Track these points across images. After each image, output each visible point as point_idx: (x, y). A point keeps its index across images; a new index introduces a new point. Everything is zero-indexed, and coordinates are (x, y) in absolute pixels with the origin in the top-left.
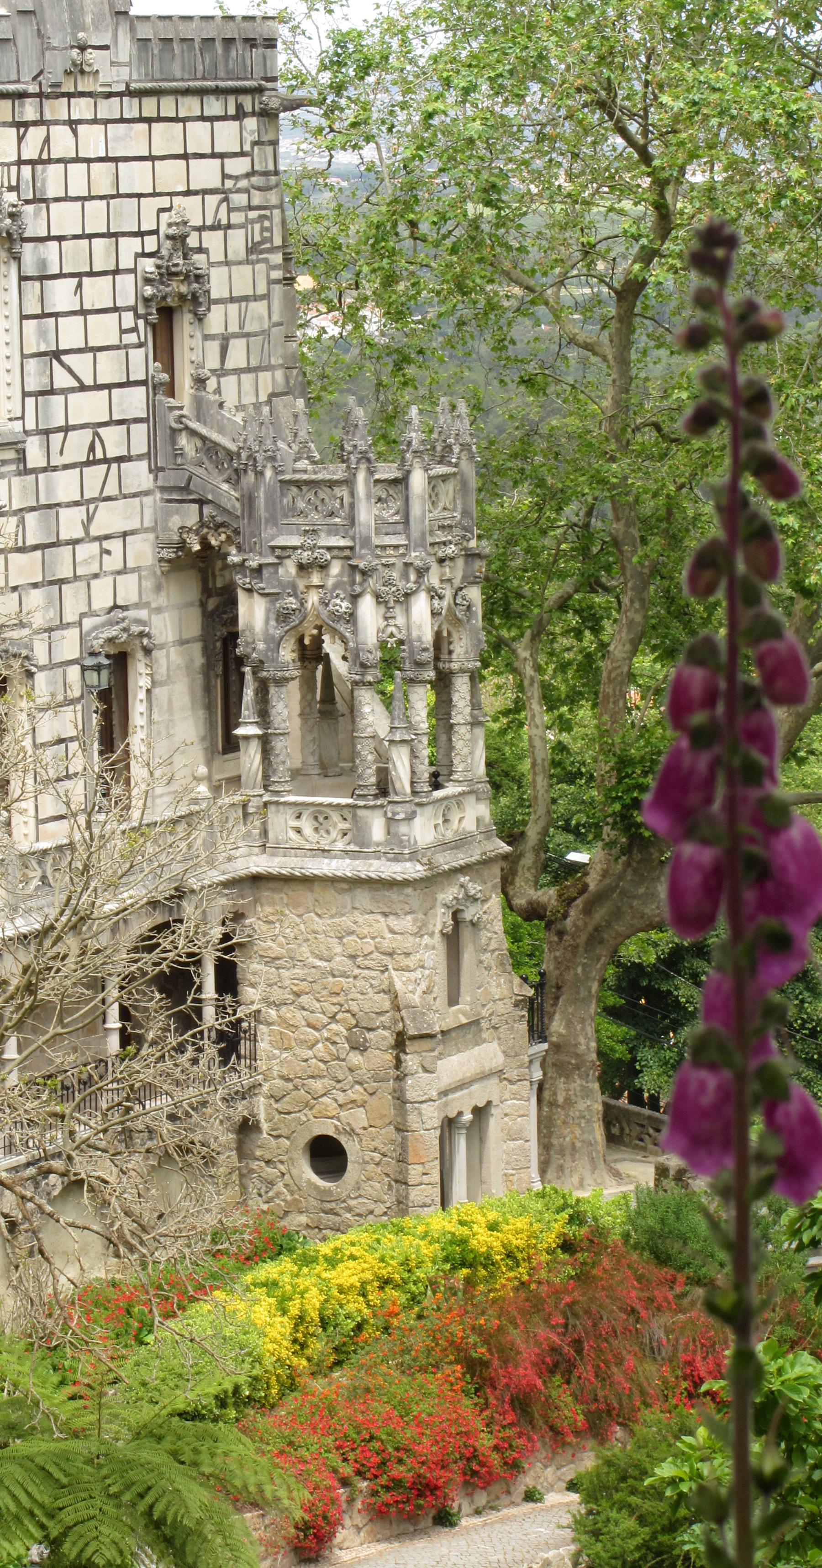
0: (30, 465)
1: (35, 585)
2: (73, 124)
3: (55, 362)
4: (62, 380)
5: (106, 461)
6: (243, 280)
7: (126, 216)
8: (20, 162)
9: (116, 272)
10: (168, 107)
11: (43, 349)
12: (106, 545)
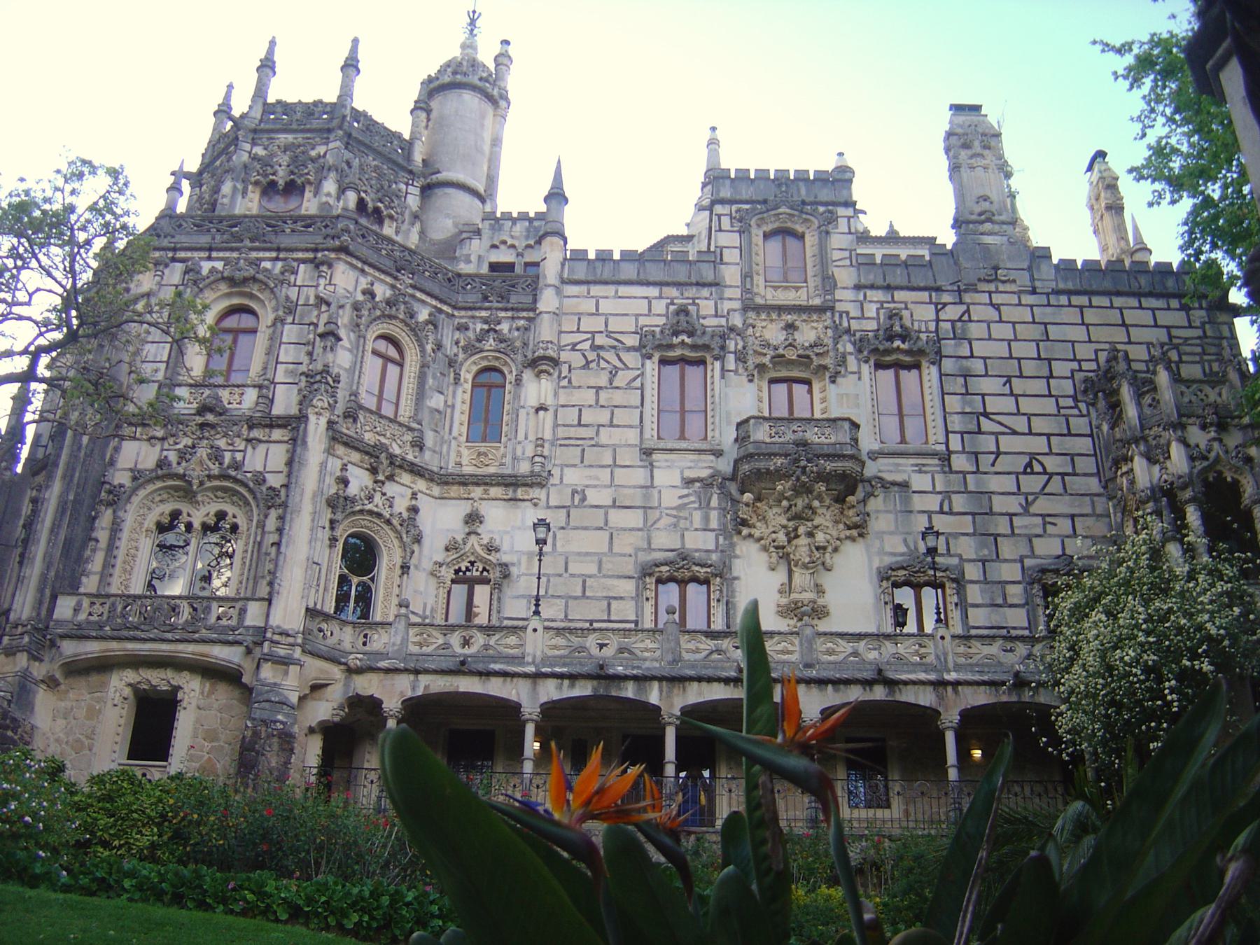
0: (954, 469)
1: (967, 534)
2: (997, 307)
3: (981, 418)
4: (986, 425)
5: (1045, 472)
8: (938, 320)
9: (1051, 376)
10: (1096, 301)
11: (968, 410)
12: (1048, 519)
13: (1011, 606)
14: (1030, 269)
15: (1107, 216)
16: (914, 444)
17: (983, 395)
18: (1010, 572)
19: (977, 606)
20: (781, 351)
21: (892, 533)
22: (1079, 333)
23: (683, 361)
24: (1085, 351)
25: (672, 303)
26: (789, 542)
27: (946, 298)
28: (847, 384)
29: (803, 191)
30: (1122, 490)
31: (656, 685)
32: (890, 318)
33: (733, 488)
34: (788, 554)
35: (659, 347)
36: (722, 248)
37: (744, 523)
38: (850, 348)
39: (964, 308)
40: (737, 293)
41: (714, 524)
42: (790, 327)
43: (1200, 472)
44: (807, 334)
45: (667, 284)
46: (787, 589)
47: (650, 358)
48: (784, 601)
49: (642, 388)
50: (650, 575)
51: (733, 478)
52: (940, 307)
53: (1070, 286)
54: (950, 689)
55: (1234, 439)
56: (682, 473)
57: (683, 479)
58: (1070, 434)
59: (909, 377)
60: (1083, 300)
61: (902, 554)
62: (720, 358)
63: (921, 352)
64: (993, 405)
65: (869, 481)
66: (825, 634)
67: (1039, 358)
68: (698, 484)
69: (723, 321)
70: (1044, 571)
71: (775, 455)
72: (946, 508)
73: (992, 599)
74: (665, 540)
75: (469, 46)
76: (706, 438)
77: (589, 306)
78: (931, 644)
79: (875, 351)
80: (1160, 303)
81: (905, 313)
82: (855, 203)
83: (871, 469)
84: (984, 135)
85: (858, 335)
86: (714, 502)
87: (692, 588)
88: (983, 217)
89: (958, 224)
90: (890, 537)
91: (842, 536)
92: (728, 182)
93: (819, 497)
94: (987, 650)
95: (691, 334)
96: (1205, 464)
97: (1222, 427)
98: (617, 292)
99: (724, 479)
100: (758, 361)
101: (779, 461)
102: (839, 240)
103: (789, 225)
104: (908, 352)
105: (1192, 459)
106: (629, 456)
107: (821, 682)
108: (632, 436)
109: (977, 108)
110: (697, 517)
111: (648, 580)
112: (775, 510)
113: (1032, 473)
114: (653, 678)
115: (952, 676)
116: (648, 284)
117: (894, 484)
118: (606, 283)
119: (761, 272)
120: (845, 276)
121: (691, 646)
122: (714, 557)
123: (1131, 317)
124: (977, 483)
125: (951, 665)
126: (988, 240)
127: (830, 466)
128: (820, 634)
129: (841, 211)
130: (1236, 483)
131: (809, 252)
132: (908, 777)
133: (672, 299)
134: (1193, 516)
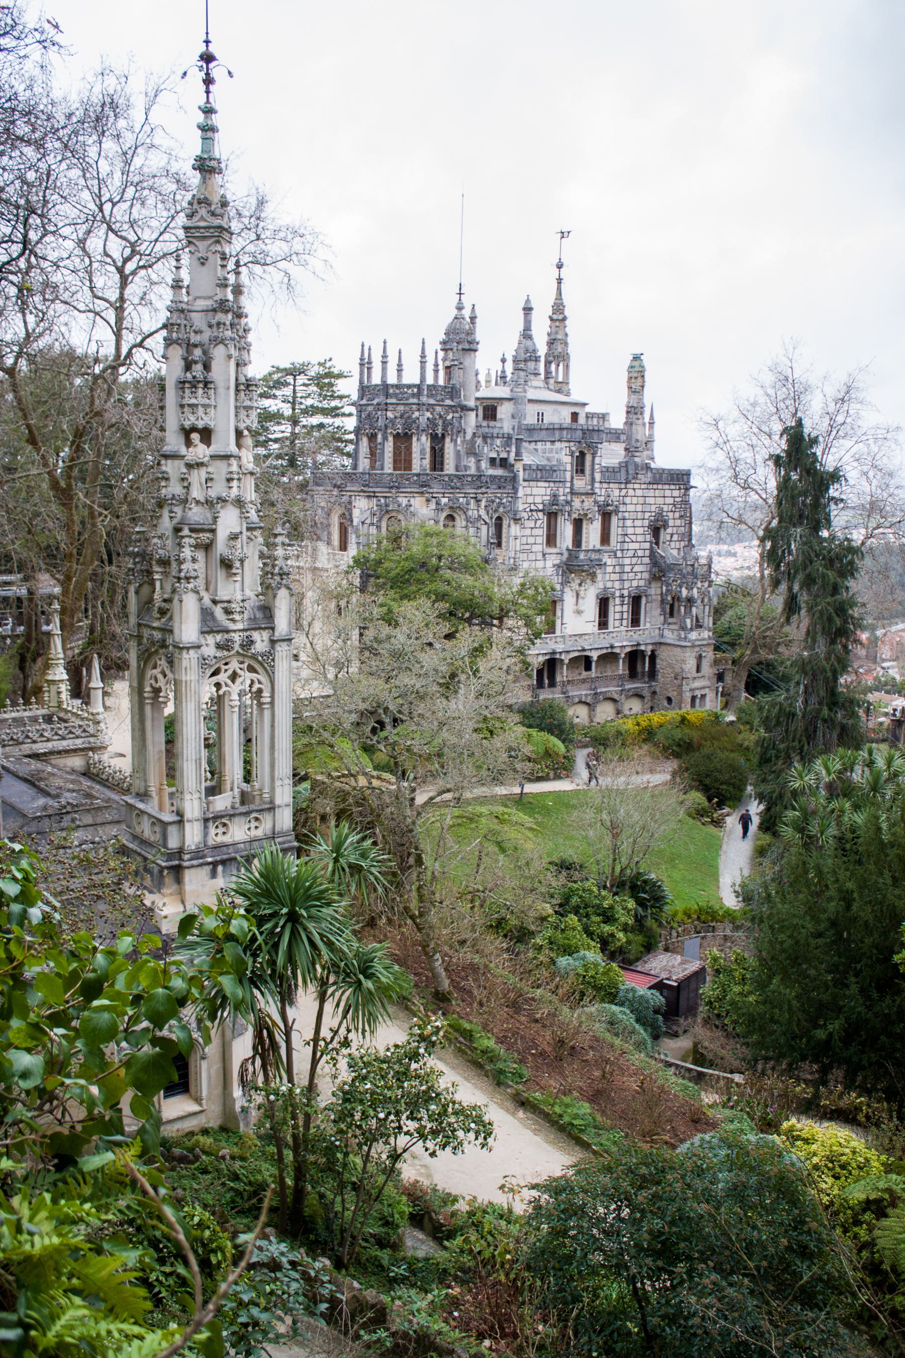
4: (627, 539)
6: (678, 522)
7: (647, 508)
10: (660, 487)
18: (626, 593)
22: (652, 500)
28: (595, 523)
40: (568, 485)
52: (621, 489)
60: (655, 486)
75: (460, 308)
77: (528, 491)
102: (597, 460)
106: (540, 556)
120: (598, 476)
123: (668, 493)
126: (636, 459)
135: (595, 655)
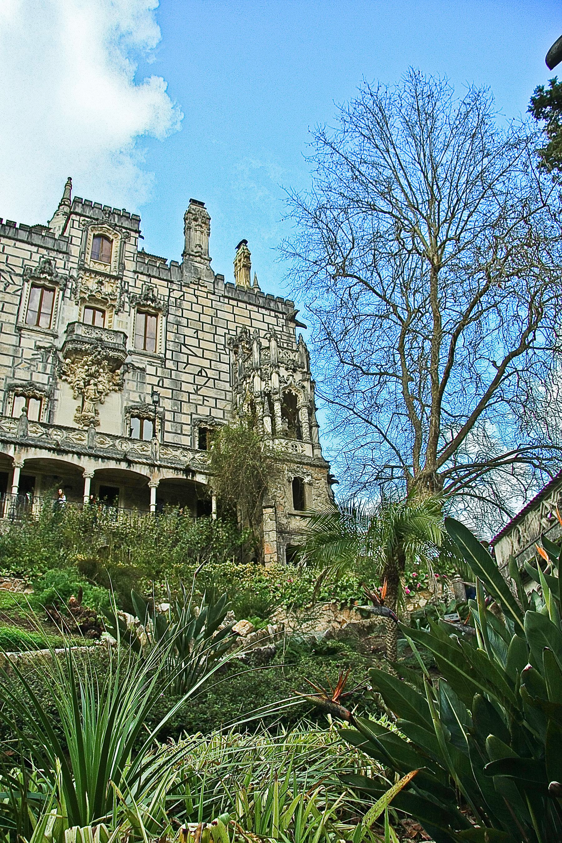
5: (207, 377)
8: (169, 296)
10: (240, 304)
11: (177, 341)
13: (184, 435)
14: (214, 283)
15: (243, 270)
16: (150, 352)
17: (185, 336)
18: (186, 419)
19: (169, 432)
20: (93, 293)
21: (134, 391)
22: (230, 317)
23: (44, 287)
24: (232, 326)
25: (43, 257)
26: (85, 386)
27: (175, 287)
28: (123, 316)
29: (116, 220)
30: (245, 390)
31: (13, 446)
32: (148, 290)
33: (60, 355)
34: (84, 392)
35: (32, 277)
36: (72, 236)
37: (64, 373)
38: (127, 300)
39: (182, 293)
41: (48, 371)
42: (101, 283)
43: (283, 389)
44: (107, 289)
45: (42, 247)
46: (81, 409)
47: (28, 281)
48: (78, 415)
49: (21, 296)
50: (13, 391)
51: (62, 350)
53: (230, 295)
54: (156, 468)
55: (298, 376)
56: (35, 342)
57: (35, 345)
58: (220, 362)
59: (151, 320)
60: (235, 303)
61: (138, 402)
62: (64, 290)
63: (160, 309)
64: (188, 341)
65: (127, 364)
66: (101, 433)
67: (212, 324)
68: (43, 350)
69: (67, 272)
70: (201, 421)
71: (86, 343)
72: (161, 385)
73: (176, 430)
74: (22, 375)
76: (49, 328)
78: (150, 446)
79: (138, 304)
80: (267, 312)
81: (155, 289)
82: (140, 232)
83: (128, 360)
84: (204, 217)
85: (132, 294)
86: (50, 360)
87: (32, 401)
88: (197, 254)
89: (184, 254)
90: (134, 392)
91: (111, 388)
92: (80, 205)
93: (103, 368)
94: (174, 453)
95: (51, 275)
96: (286, 385)
97: (294, 371)
98: (15, 244)
99: (56, 350)
100: (83, 295)
101: (88, 346)
103: (107, 234)
104: (154, 308)
105: (280, 382)
106: (11, 329)
107: (97, 457)
108: (13, 319)
109: (202, 204)
110: (41, 365)
111: (11, 393)
112: (80, 370)
113: (201, 376)
114: (12, 443)
115: (158, 463)
116: (32, 244)
117: (138, 368)
118: (10, 238)
119: (90, 253)
120: (130, 265)
121: (34, 429)
122: (46, 387)
124: (176, 376)
125: (158, 458)
126: (197, 265)
127: (111, 354)
128: (98, 433)
129: (133, 234)
130: (297, 396)
131: (114, 250)
132: (128, 507)
133: (43, 255)
134: (277, 407)
135: (90, 467)
